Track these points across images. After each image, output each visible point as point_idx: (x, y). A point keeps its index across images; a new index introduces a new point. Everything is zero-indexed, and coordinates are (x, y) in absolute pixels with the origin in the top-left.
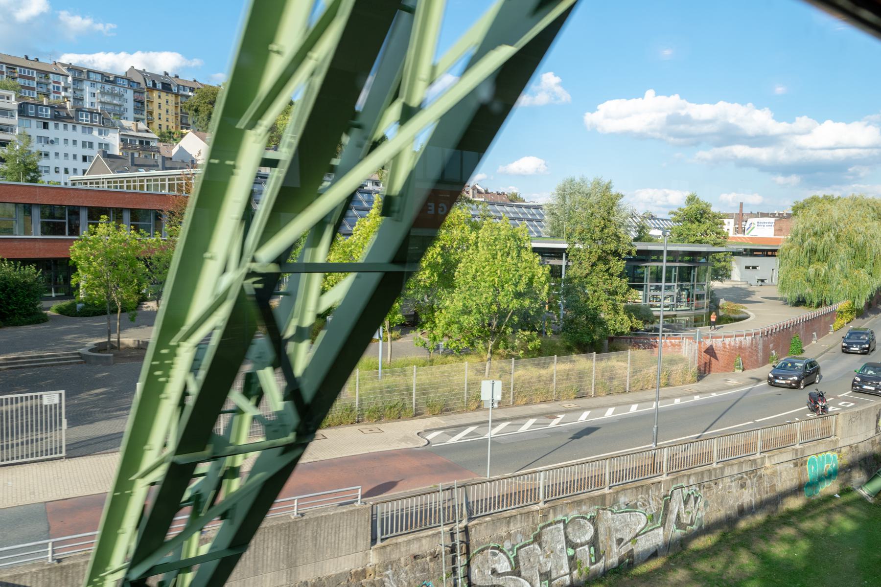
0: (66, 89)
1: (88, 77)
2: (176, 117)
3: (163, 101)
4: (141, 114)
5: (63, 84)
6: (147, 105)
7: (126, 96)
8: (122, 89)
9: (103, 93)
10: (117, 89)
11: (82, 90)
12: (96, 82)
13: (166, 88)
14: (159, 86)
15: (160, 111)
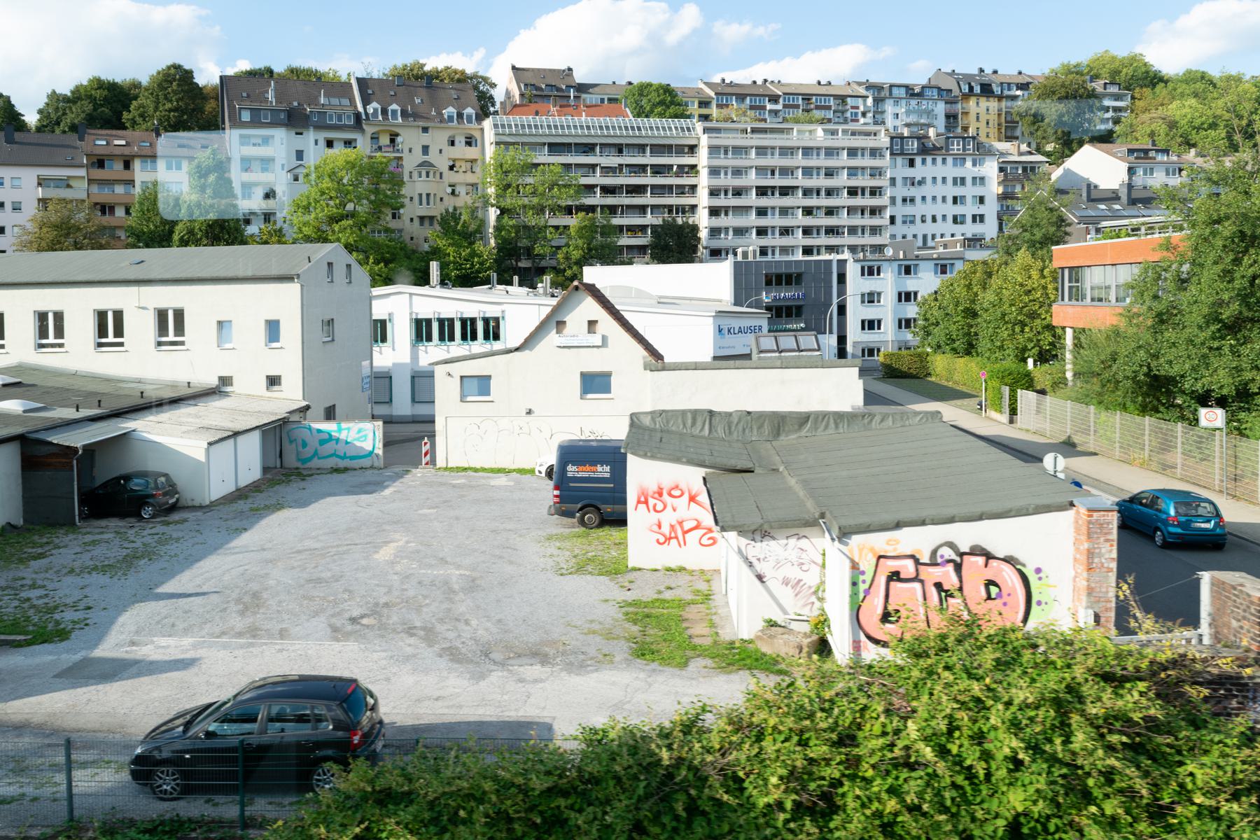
0: (864, 114)
1: (891, 93)
5: (862, 108)
8: (931, 102)
9: (908, 113)
11: (883, 112)
12: (901, 98)
13: (987, 90)
14: (977, 89)
15: (978, 125)
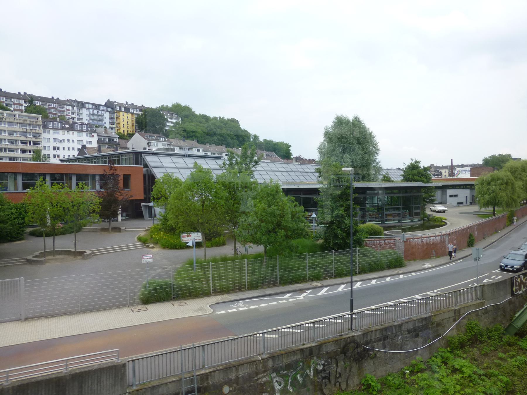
2: (132, 126)
3: (125, 118)
4: (114, 125)
6: (117, 120)
7: (105, 115)
8: (103, 112)
10: (100, 112)
13: (127, 110)
14: (123, 109)
15: (123, 123)
